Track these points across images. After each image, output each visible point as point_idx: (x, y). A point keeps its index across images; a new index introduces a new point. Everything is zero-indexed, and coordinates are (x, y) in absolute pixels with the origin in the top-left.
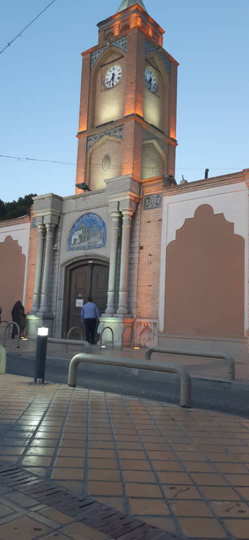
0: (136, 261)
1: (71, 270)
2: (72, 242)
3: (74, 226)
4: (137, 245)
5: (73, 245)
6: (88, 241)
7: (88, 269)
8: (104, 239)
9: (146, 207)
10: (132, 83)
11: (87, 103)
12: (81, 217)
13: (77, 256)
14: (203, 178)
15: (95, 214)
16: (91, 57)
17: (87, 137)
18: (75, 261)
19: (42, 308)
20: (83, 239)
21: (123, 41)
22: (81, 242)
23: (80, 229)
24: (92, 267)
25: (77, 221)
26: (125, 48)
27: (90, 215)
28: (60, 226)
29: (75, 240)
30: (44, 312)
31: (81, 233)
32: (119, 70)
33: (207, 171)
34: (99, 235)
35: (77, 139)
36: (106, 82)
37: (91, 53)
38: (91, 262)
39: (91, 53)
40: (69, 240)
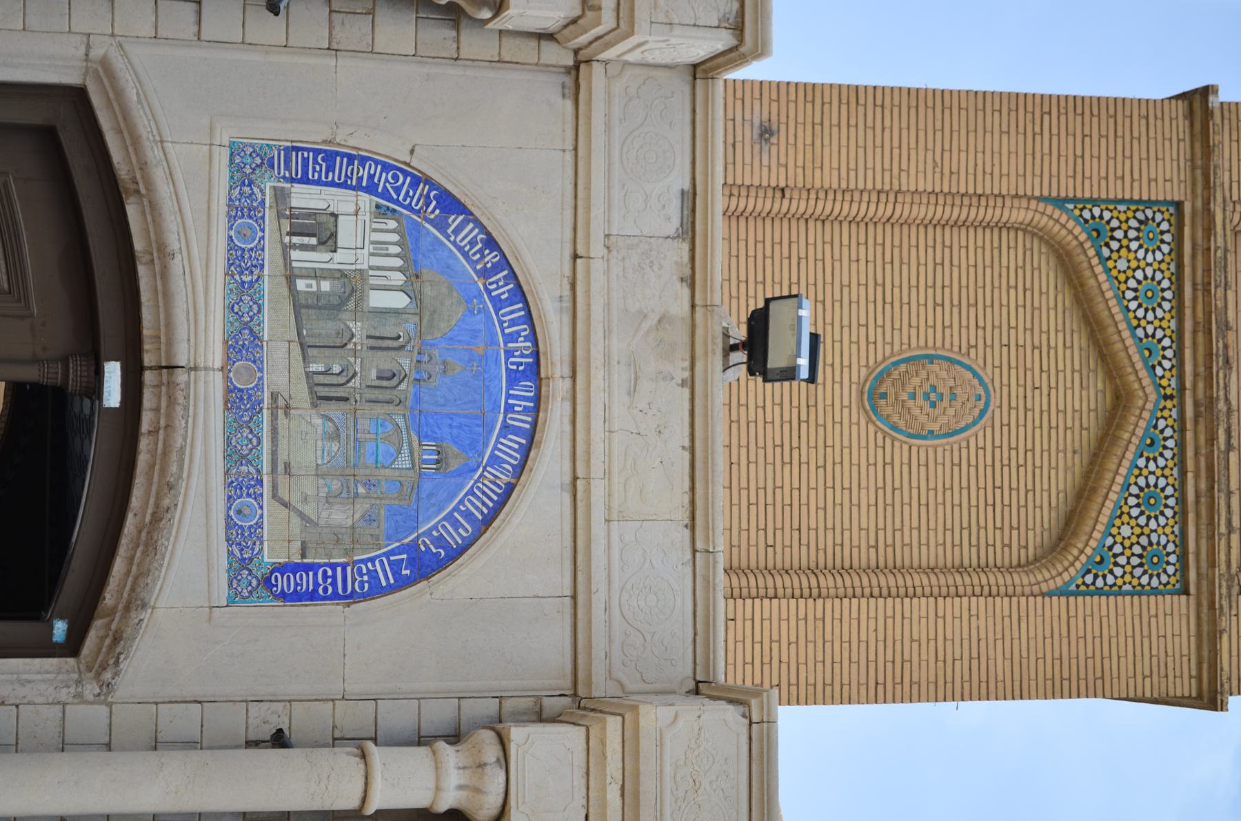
1: (48, 137)
2: (305, 197)
3: (450, 204)
5: (281, 196)
6: (301, 393)
12: (519, 294)
13: (176, 266)
15: (526, 451)
17: (1179, 205)
20: (324, 328)
22: (300, 305)
23: (416, 297)
25: (491, 243)
27: (525, 389)
29: (323, 231)
31: (378, 300)
34: (339, 516)
38: (112, 396)
40: (328, 163)
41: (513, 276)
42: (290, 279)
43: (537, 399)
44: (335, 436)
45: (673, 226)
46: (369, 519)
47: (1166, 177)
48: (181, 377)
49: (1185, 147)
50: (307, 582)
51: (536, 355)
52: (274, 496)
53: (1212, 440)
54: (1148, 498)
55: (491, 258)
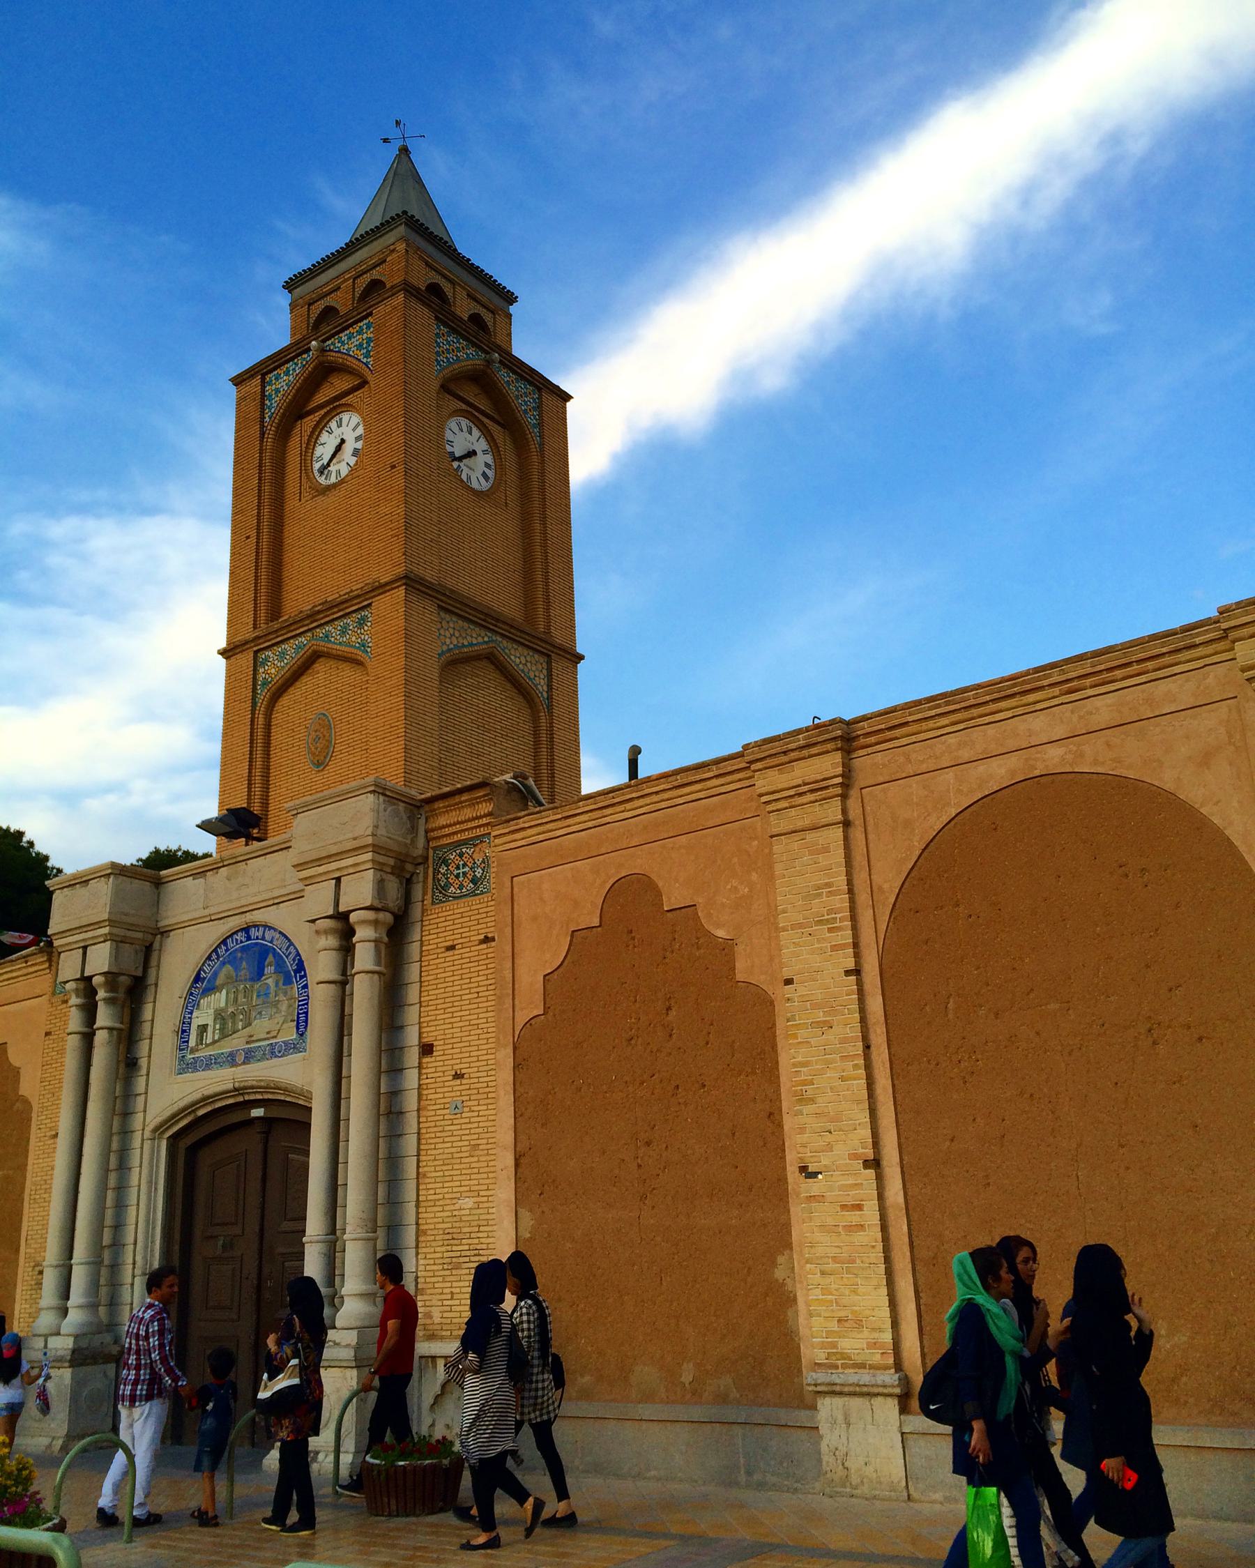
0: (410, 1102)
1: (193, 1150)
3: (198, 979)
4: (411, 1038)
7: (250, 1142)
8: (302, 1022)
9: (442, 892)
10: (393, 467)
11: (253, 540)
12: (224, 942)
13: (207, 1093)
14: (623, 778)
15: (270, 928)
16: (263, 387)
17: (256, 652)
18: (201, 1113)
19: (76, 1317)
21: (360, 332)
24: (267, 1134)
25: (209, 958)
26: (367, 355)
27: (253, 932)
28: (151, 979)
30: (76, 1337)
31: (223, 1004)
32: (358, 424)
33: (635, 752)
34: (284, 1007)
35: (222, 662)
36: (317, 466)
37: (264, 376)
38: (257, 1112)
39: (264, 376)
41: (219, 946)
42: (214, 1042)
43: (255, 926)
44: (260, 1013)
45: (202, 880)
46: (285, 993)
47: (246, 659)
48: (237, 1085)
49: (238, 656)
50: (302, 1018)
51: (242, 930)
52: (275, 1037)
53: (319, 612)
54: (343, 632)
55: (214, 956)
